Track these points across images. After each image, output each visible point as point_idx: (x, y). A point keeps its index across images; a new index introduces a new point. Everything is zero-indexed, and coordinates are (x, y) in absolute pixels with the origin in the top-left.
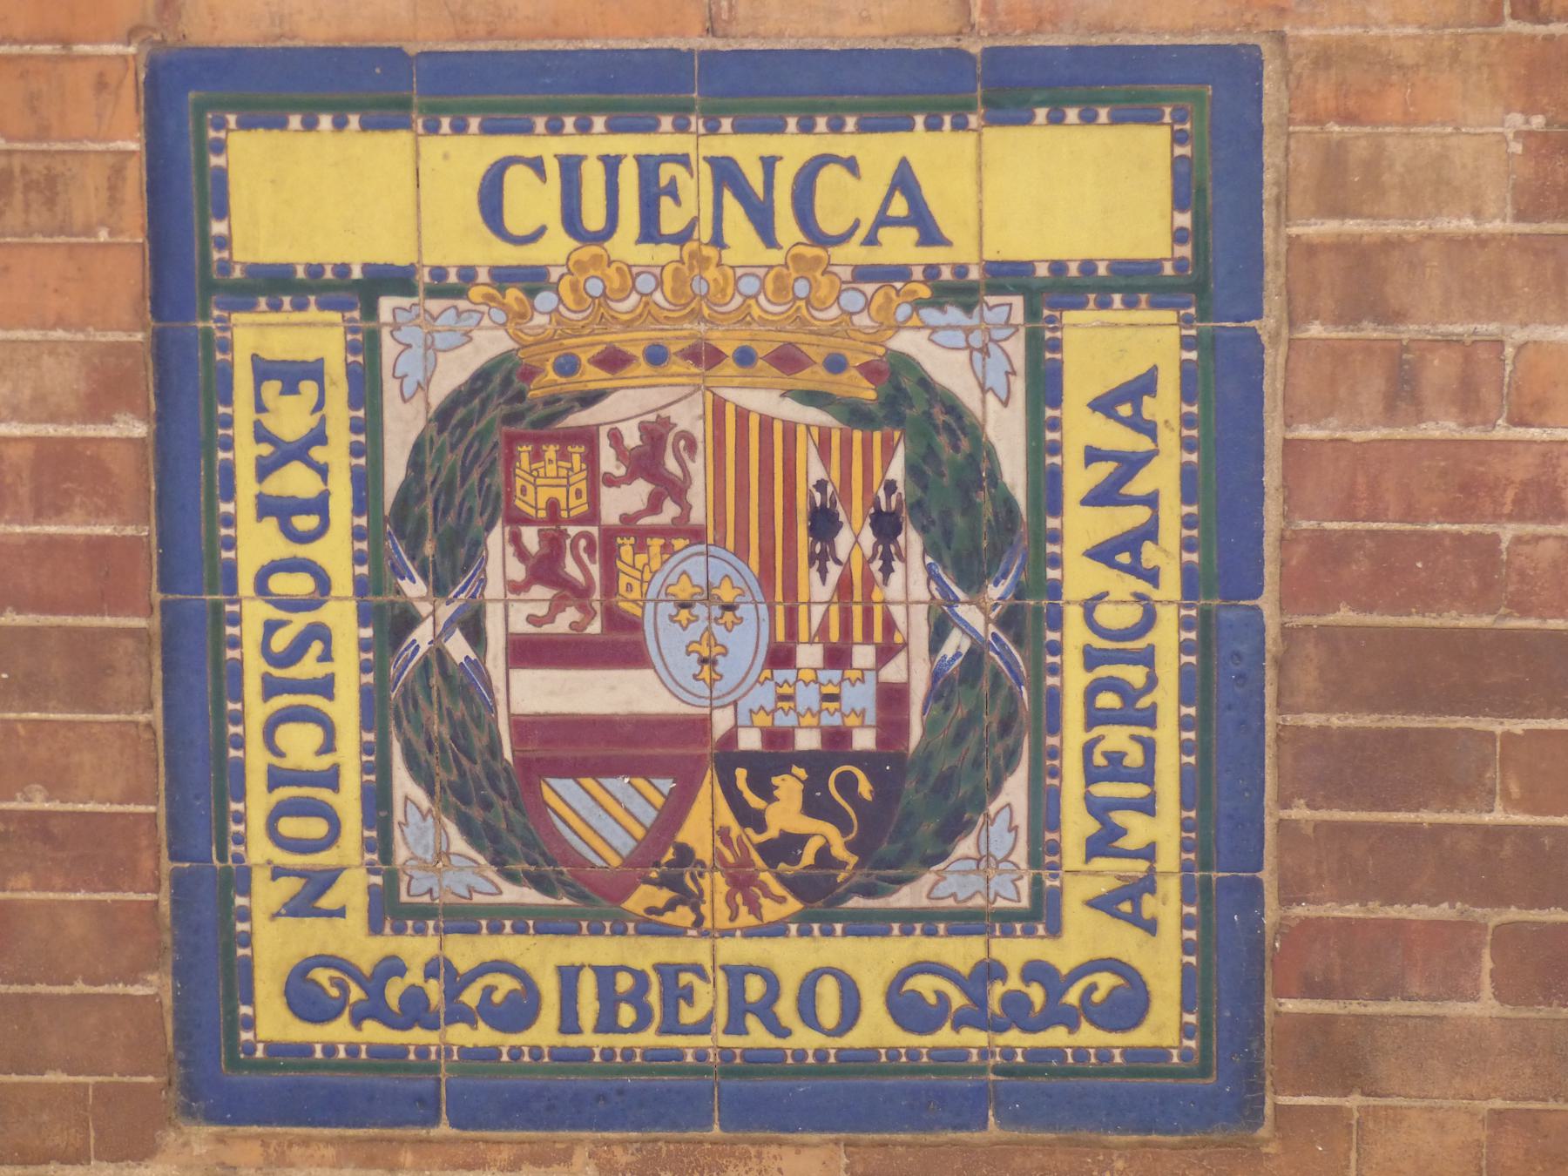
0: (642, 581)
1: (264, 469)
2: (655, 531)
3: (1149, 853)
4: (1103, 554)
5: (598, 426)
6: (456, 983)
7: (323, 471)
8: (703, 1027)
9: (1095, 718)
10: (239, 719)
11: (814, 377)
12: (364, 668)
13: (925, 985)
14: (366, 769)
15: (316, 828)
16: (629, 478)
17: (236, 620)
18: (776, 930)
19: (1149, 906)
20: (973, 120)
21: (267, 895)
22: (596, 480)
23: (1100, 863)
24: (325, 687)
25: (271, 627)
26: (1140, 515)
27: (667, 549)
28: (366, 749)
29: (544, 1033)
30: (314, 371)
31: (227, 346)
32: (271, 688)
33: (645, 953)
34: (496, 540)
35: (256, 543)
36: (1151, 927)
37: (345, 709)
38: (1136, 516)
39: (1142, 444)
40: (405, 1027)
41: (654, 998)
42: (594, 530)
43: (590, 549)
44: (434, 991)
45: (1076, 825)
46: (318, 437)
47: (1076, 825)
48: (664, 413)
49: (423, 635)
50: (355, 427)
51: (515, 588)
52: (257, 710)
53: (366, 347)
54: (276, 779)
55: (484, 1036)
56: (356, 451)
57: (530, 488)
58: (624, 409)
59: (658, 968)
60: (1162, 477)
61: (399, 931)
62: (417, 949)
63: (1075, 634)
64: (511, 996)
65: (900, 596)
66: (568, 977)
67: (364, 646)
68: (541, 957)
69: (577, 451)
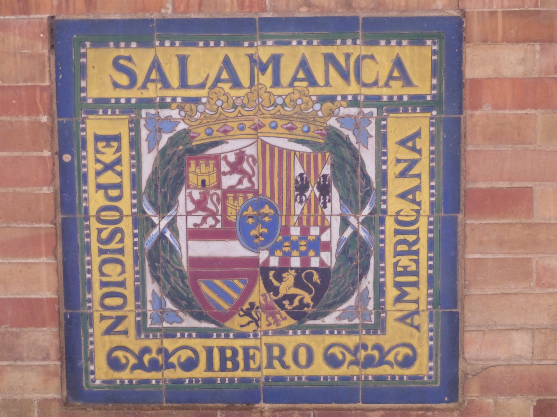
0: (236, 210)
1: (98, 174)
2: (241, 191)
3: (417, 301)
4: (403, 196)
5: (221, 154)
6: (168, 355)
7: (120, 174)
8: (259, 369)
9: (397, 254)
10: (90, 263)
11: (298, 133)
12: (135, 244)
13: (336, 351)
14: (136, 280)
15: (117, 301)
16: (231, 173)
17: (88, 227)
18: (282, 332)
19: (417, 320)
20: (358, 42)
21: (99, 327)
22: (220, 174)
23: (400, 306)
24: (121, 251)
25: (100, 231)
26: (414, 182)
27: (245, 198)
28: (137, 273)
29: (200, 372)
30: (117, 138)
31: (84, 130)
32: (101, 252)
33: (239, 343)
34: (181, 197)
35: (95, 200)
36: (418, 328)
37: (128, 259)
38: (414, 182)
39: (416, 156)
40: (149, 370)
41: (240, 358)
42: (219, 192)
43: (218, 200)
44: (160, 358)
45: (392, 292)
46: (118, 161)
47: (392, 292)
48: (243, 150)
49: (155, 232)
50: (132, 157)
51: (189, 213)
52: (96, 260)
53: (135, 128)
54: (103, 284)
55: (179, 373)
56: (133, 166)
57: (196, 177)
58: (229, 149)
59: (241, 347)
60: (423, 167)
61: (147, 337)
62: (153, 344)
63: (390, 225)
64: (189, 359)
65: (330, 214)
66: (209, 351)
67: (135, 235)
68: (198, 344)
69: (212, 162)
